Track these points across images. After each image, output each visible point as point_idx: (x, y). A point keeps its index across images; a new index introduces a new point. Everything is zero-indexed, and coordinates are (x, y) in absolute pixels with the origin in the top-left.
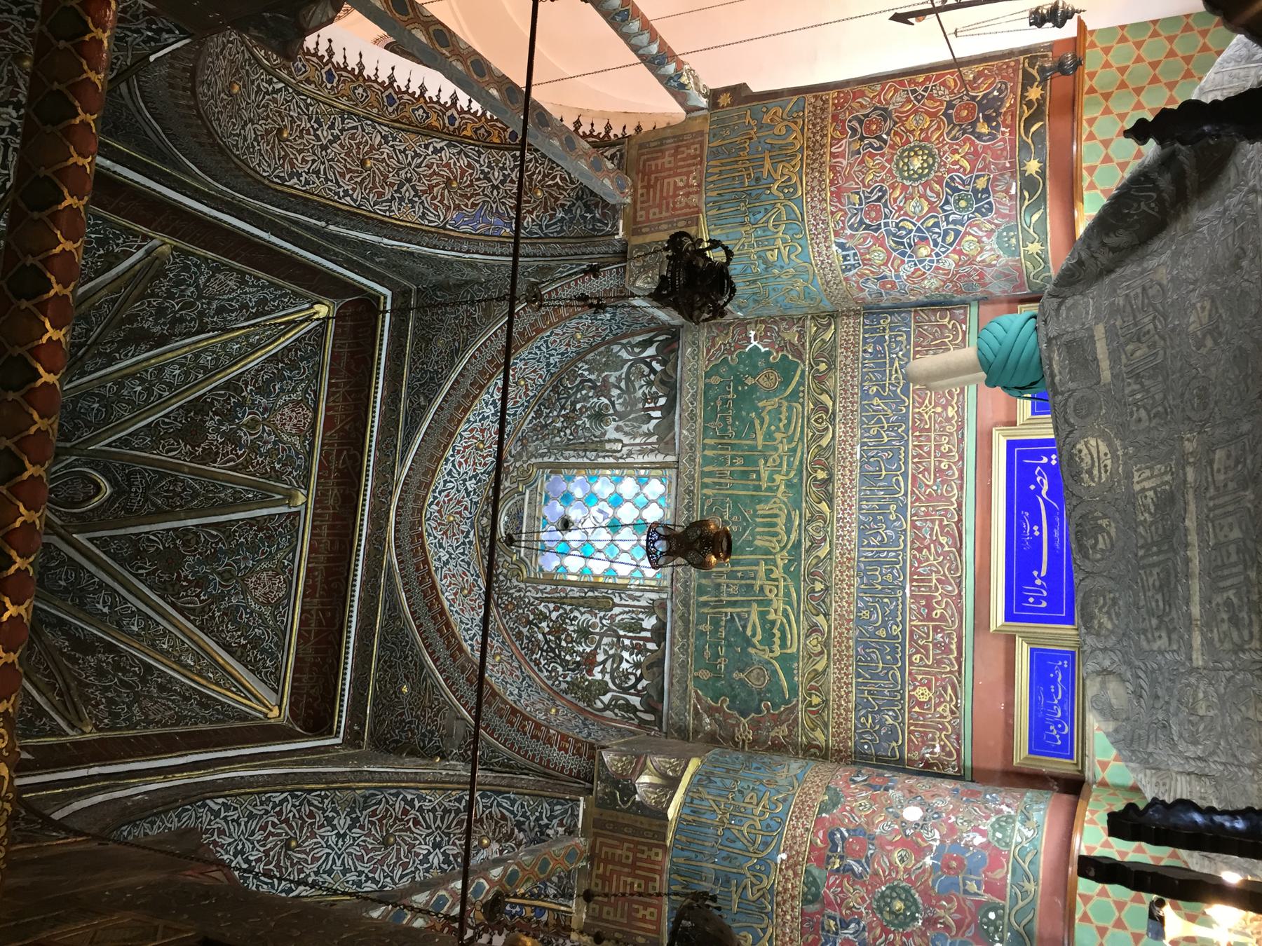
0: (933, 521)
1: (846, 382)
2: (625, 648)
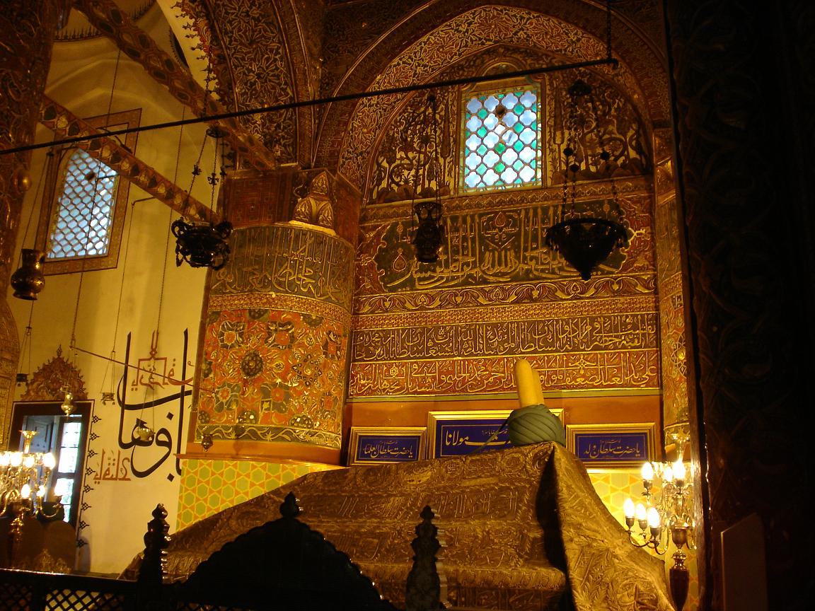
0: (502, 373)
2: (417, 171)
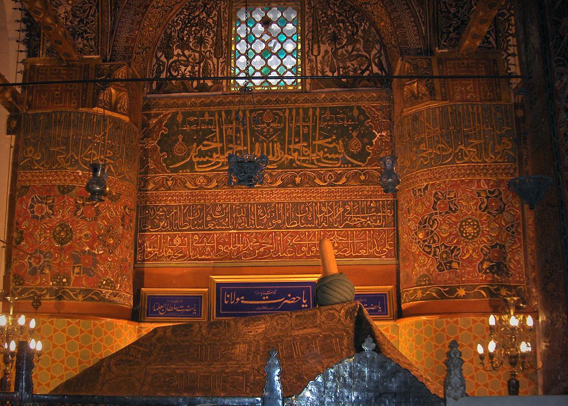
0: (271, 244)
1: (353, 192)
2: (193, 67)
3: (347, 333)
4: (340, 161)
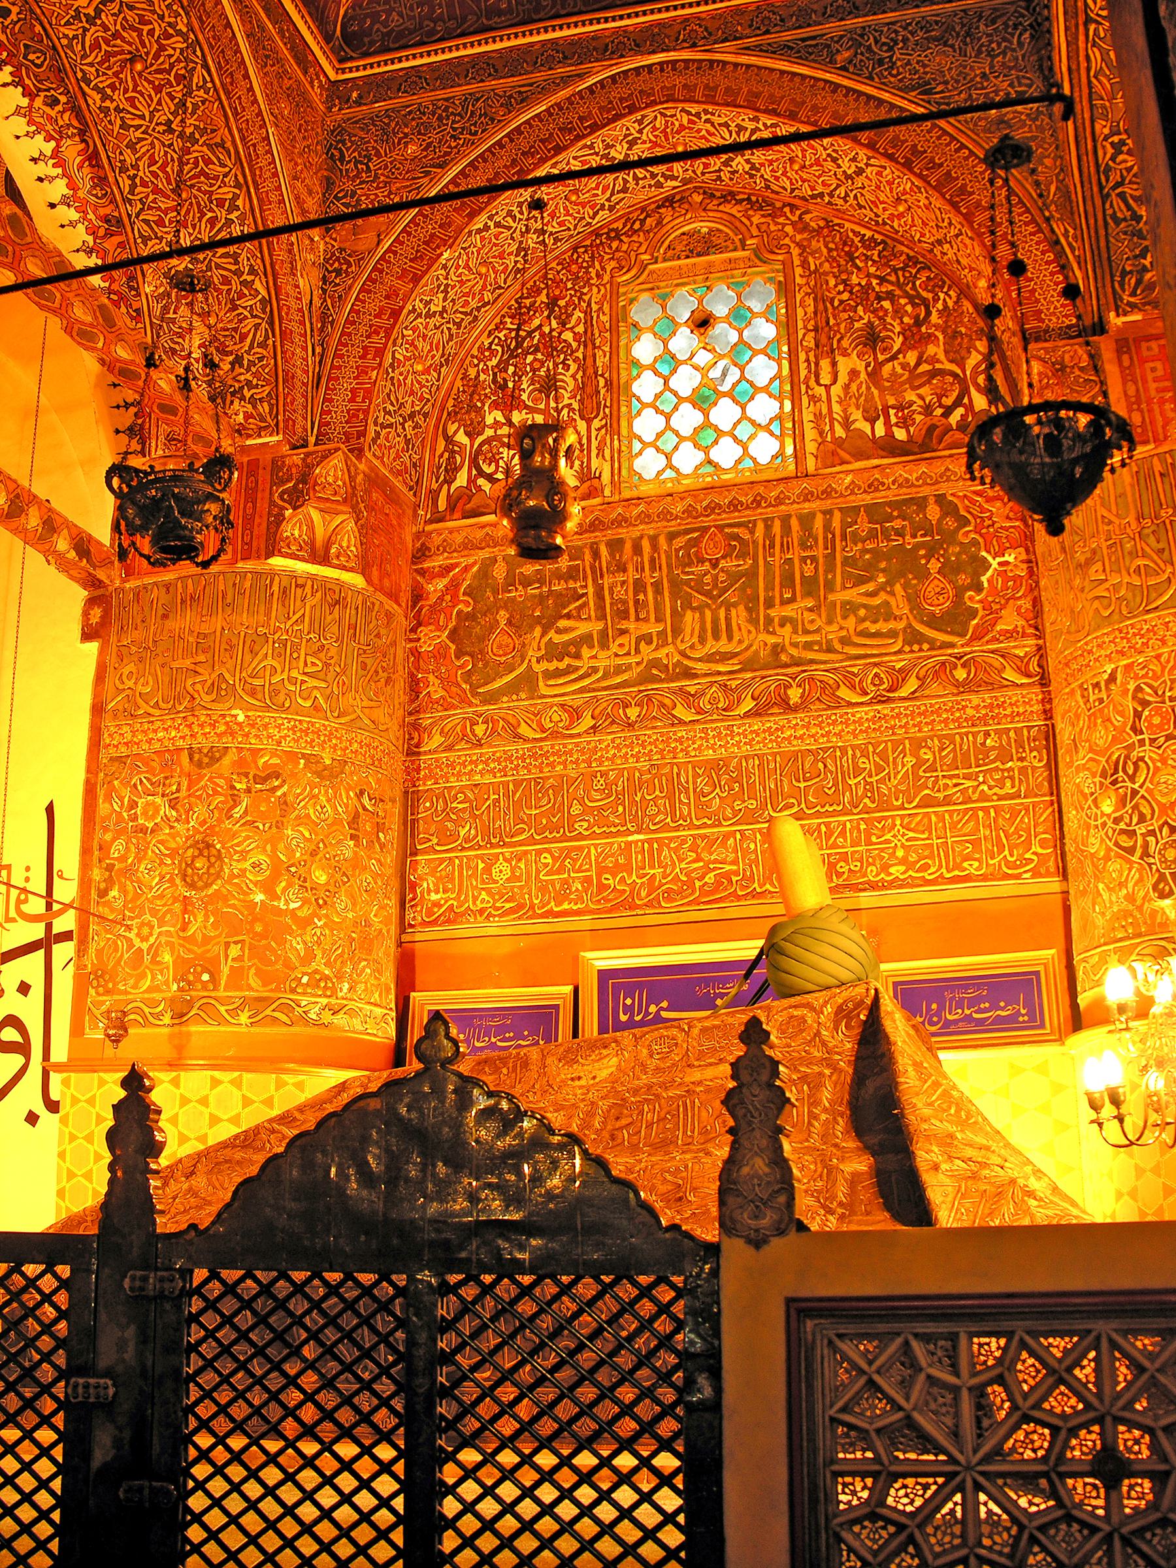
0: (733, 863)
1: (937, 712)
3: (835, 1068)
4: (901, 639)
